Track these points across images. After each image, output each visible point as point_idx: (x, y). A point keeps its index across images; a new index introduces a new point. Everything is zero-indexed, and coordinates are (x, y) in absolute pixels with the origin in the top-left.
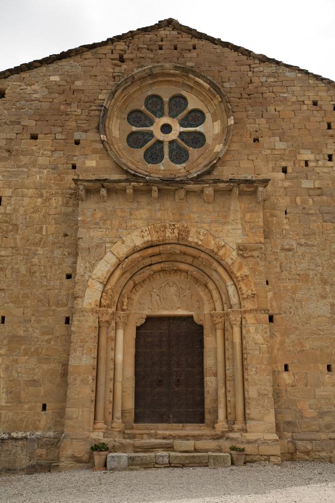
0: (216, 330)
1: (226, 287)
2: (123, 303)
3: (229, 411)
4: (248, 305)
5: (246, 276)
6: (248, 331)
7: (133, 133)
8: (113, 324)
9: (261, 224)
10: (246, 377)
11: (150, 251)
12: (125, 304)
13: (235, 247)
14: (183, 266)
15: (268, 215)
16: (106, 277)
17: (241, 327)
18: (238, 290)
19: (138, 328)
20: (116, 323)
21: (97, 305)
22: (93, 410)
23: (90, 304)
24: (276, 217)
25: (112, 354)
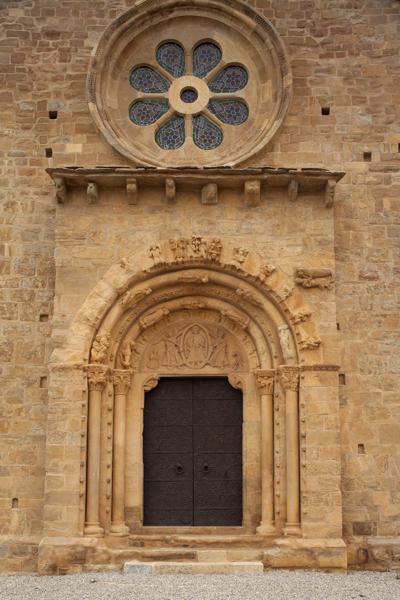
0: (261, 396)
1: (277, 332)
2: (124, 356)
3: (277, 509)
4: (310, 360)
5: (307, 316)
6: (307, 398)
7: (138, 102)
8: (110, 387)
9: (331, 237)
10: (303, 462)
11: (163, 279)
12: (127, 358)
13: (292, 272)
14: (212, 303)
15: (342, 225)
17: (298, 393)
18: (294, 336)
19: (148, 395)
20: (114, 386)
21: (85, 360)
22: (83, 507)
23: (74, 357)
24: (353, 229)
25: (108, 432)
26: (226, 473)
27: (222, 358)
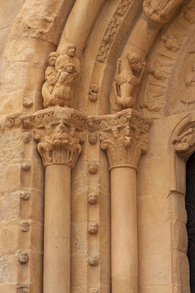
16: (46, 21)
20: (105, 152)
21: (28, 107)
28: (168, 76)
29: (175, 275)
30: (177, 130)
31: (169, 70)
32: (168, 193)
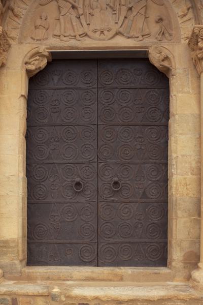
26: (144, 193)
27: (140, 23)
28: (23, 17)
29: (20, 150)
30: (29, 55)
31: (24, 12)
32: (19, 96)
